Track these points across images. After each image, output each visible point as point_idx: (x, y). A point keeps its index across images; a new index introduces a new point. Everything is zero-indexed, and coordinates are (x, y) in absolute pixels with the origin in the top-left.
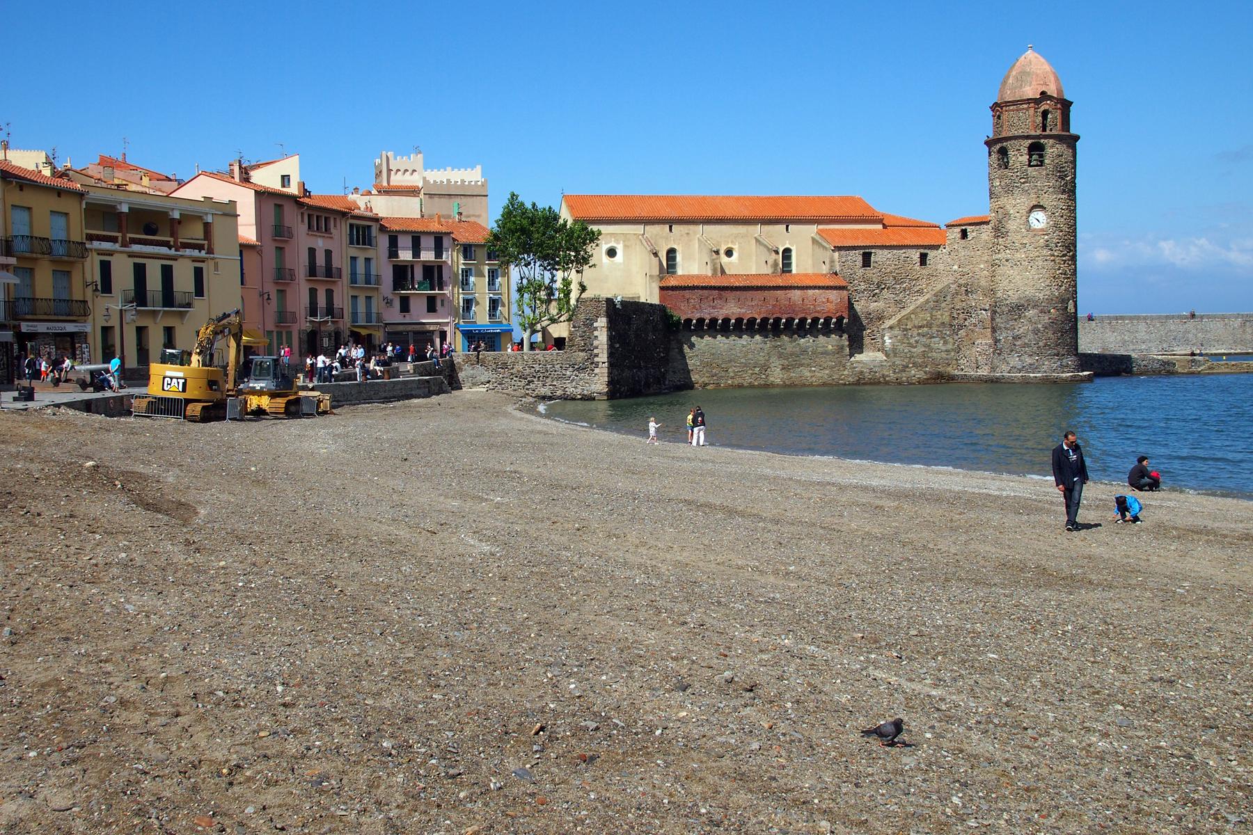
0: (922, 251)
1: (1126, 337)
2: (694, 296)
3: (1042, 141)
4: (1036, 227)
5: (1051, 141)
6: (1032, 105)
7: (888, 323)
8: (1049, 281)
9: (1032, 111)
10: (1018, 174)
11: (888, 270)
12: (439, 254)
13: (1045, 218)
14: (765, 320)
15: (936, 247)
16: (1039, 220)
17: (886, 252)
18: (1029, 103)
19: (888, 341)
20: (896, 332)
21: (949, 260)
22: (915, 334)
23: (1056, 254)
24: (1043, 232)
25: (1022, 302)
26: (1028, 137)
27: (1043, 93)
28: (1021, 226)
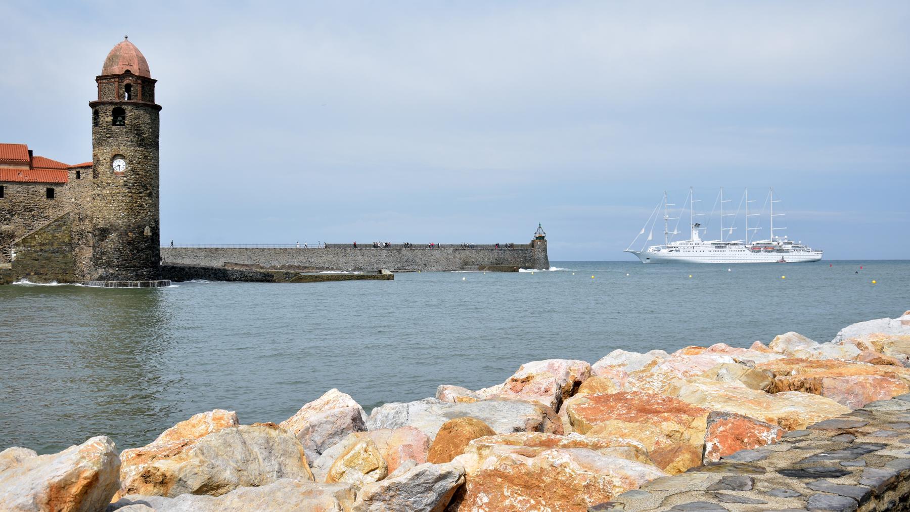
0: (49, 187)
1: (372, 259)
3: (123, 107)
4: (118, 171)
5: (130, 107)
6: (117, 79)
7: (17, 240)
8: (127, 211)
9: (116, 84)
10: (105, 130)
11: (18, 201)
13: (125, 164)
15: (62, 184)
16: (120, 165)
17: (16, 187)
18: (115, 78)
19: (13, 255)
20: (21, 248)
21: (69, 194)
22: (38, 249)
23: (133, 191)
25: (107, 227)
26: (111, 103)
27: (128, 72)
28: (107, 170)
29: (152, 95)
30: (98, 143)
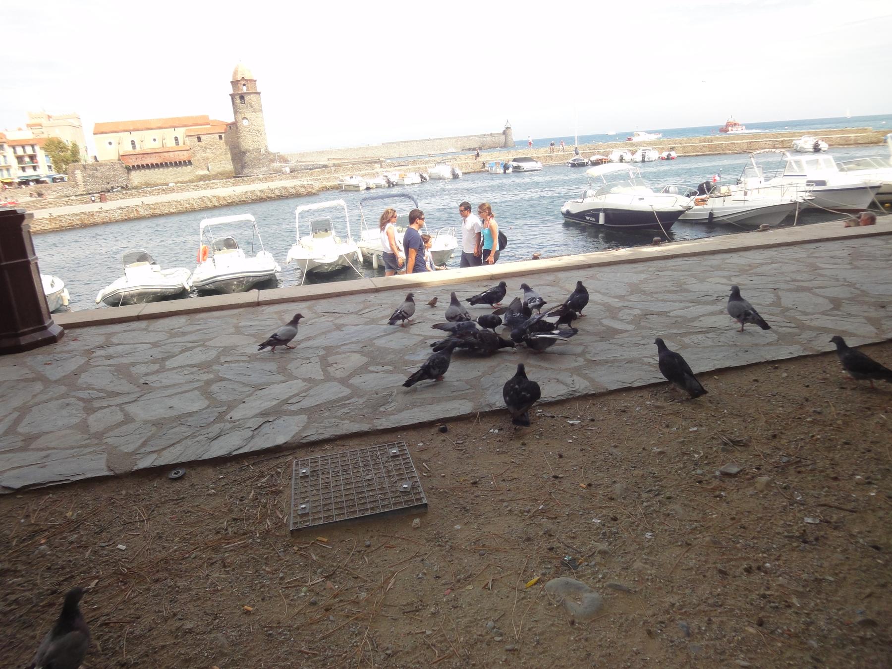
2: (134, 158)
12: (34, 151)
14: (161, 164)
19: (209, 167)
24: (248, 126)
29: (255, 87)
30: (236, 112)
